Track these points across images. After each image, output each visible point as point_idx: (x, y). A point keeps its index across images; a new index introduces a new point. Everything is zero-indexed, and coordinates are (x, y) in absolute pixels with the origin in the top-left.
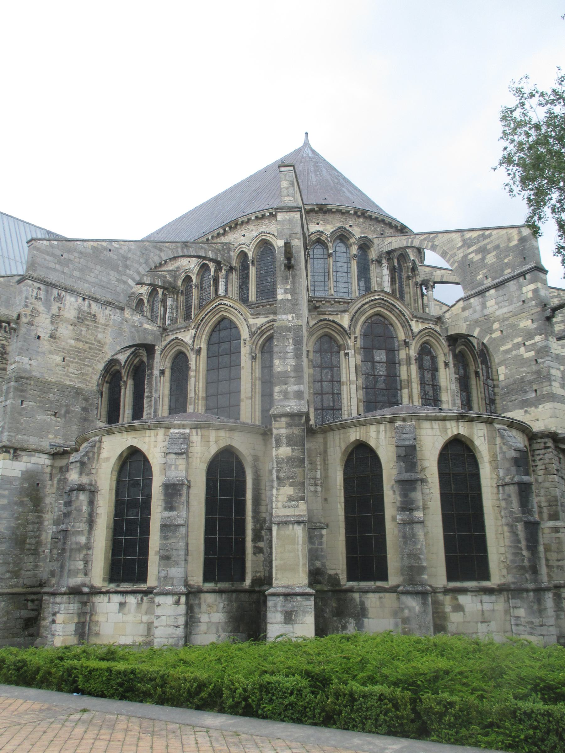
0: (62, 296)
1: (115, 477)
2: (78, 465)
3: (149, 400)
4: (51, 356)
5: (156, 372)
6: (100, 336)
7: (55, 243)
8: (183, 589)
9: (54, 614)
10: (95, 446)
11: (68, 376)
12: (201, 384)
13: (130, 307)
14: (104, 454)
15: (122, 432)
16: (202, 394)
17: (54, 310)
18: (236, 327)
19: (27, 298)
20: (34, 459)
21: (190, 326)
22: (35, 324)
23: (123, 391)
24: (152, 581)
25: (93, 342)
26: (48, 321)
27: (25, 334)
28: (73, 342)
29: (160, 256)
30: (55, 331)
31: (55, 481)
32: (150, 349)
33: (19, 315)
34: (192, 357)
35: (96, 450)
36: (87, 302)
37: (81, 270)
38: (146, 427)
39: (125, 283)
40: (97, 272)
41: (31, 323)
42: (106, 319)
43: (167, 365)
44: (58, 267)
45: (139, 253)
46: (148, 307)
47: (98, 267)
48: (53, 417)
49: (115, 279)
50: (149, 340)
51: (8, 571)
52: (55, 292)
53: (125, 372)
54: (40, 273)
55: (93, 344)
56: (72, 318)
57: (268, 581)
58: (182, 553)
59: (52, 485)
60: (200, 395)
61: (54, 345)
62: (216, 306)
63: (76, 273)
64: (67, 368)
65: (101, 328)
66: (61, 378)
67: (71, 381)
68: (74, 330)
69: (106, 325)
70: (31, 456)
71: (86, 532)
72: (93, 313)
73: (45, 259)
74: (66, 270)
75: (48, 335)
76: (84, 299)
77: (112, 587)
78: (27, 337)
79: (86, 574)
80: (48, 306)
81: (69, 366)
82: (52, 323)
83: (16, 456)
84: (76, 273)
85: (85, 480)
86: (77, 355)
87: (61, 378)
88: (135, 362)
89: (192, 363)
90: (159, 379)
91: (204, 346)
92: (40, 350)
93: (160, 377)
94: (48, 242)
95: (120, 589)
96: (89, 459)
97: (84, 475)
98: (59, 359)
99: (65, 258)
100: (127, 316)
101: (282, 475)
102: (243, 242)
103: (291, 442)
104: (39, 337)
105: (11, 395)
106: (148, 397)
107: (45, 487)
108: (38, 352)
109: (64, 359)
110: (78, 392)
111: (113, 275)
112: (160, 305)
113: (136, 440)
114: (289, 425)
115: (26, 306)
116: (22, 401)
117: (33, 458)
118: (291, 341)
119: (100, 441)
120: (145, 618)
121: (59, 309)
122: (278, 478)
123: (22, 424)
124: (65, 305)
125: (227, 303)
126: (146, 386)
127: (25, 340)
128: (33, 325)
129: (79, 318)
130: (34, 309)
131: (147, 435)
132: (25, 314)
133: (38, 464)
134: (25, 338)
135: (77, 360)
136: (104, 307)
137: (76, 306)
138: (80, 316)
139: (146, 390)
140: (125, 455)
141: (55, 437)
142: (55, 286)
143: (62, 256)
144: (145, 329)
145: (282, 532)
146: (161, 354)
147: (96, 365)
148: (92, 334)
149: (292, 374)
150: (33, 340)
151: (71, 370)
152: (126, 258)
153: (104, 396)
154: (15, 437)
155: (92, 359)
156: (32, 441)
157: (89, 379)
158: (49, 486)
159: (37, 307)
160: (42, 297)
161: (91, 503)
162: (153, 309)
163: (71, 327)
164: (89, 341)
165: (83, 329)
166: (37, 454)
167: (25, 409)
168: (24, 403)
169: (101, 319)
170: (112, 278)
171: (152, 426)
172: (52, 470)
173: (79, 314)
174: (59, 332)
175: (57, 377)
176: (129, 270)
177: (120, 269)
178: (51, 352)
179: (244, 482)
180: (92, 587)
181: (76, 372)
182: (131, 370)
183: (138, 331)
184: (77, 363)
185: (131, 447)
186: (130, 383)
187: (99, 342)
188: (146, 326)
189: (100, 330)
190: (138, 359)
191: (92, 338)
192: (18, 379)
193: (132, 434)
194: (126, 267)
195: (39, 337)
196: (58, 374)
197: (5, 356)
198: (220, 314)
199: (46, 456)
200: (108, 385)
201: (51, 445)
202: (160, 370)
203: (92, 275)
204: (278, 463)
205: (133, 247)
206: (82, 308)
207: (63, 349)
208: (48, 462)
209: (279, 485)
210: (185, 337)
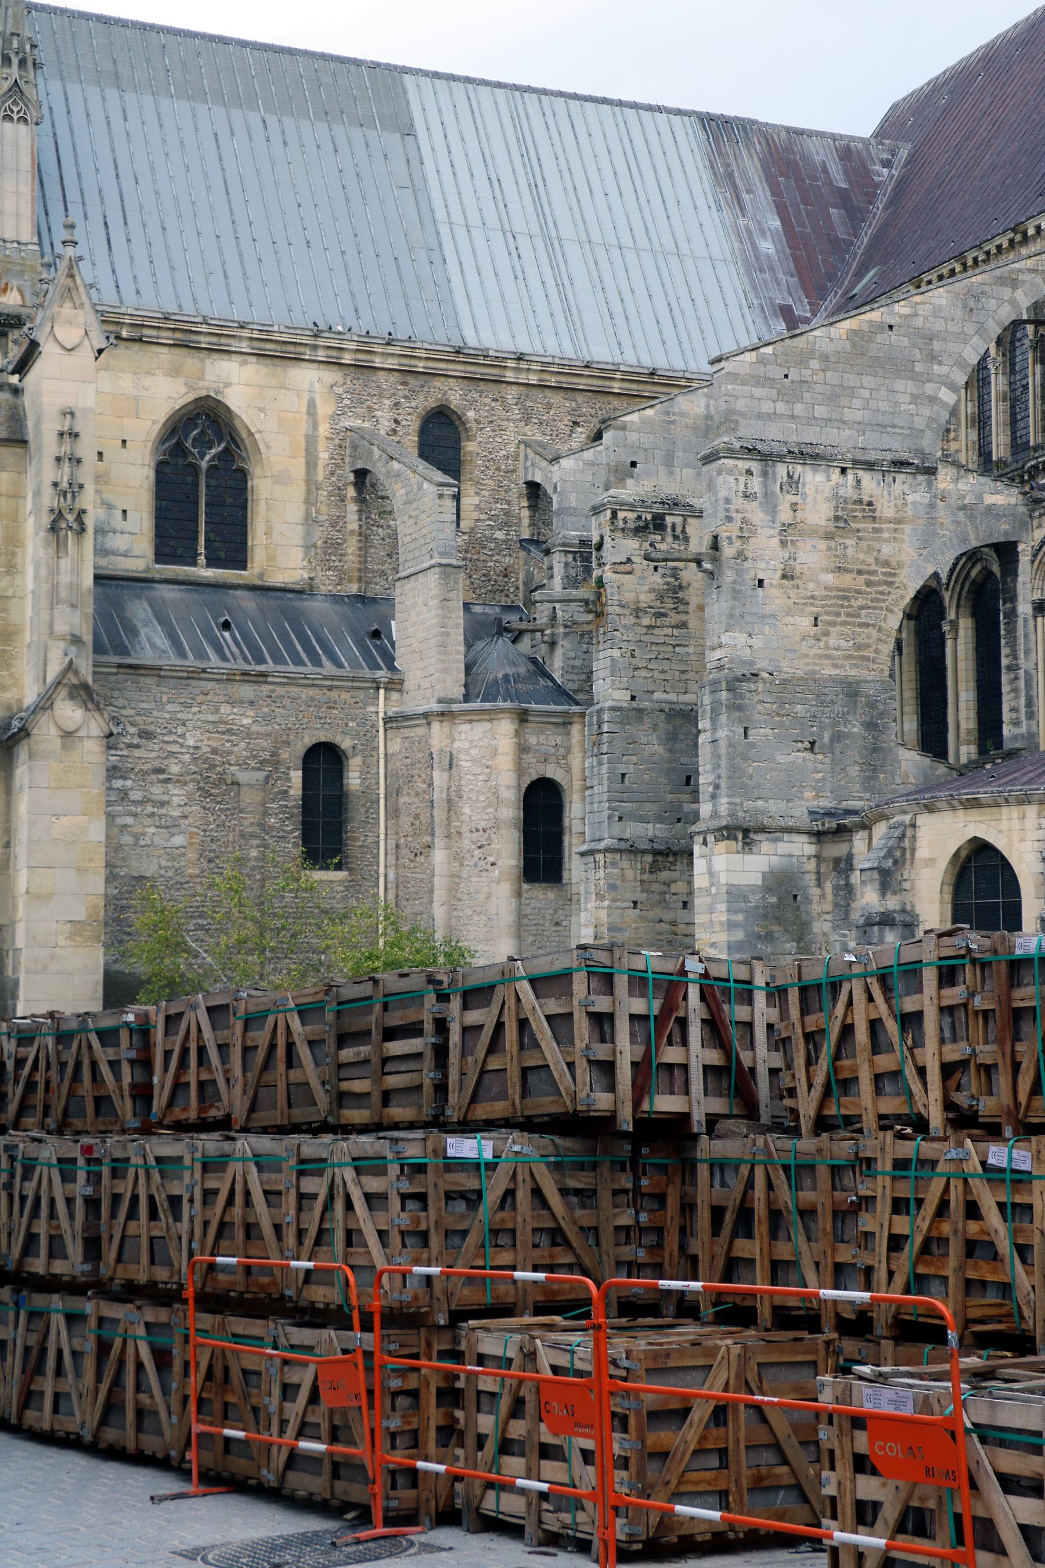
0: (796, 477)
1: (948, 898)
2: (876, 875)
3: (1012, 676)
4: (789, 619)
6: (887, 549)
7: (769, 350)
10: (904, 836)
13: (949, 459)
14: (923, 852)
15: (954, 809)
17: (785, 515)
20: (782, 847)
22: (749, 555)
23: (949, 644)
25: (874, 567)
26: (775, 542)
27: (734, 582)
28: (830, 578)
29: (1013, 302)
30: (791, 562)
31: (828, 887)
32: (1007, 551)
33: (716, 537)
35: (907, 844)
36: (850, 476)
37: (832, 399)
38: (1001, 800)
39: (933, 399)
41: (741, 556)
42: (896, 506)
44: (781, 407)
45: (959, 313)
46: (1000, 359)
47: (868, 381)
48: (808, 755)
49: (908, 398)
50: (1002, 530)
52: (781, 470)
53: (951, 597)
54: (749, 431)
55: (873, 573)
56: (823, 523)
59: (823, 896)
61: (793, 593)
63: (820, 411)
64: (824, 639)
65: (888, 530)
66: (815, 664)
67: (835, 666)
68: (829, 549)
69: (898, 521)
70: (775, 840)
72: (866, 499)
73: (752, 397)
74: (799, 409)
75: (779, 573)
76: (843, 471)
78: (737, 587)
80: (770, 504)
81: (827, 634)
83: (748, 844)
84: (820, 411)
85: (892, 903)
86: (842, 606)
87: (815, 664)
88: (973, 574)
90: (1031, 622)
92: (768, 610)
93: (1035, 618)
94: (754, 353)
96: (895, 862)
97: (889, 896)
98: (806, 622)
99: (792, 382)
100: (942, 486)
104: (761, 583)
106: (1010, 668)
107: (808, 900)
108: (764, 617)
109: (816, 619)
110: (852, 690)
111: (904, 386)
112: (1030, 360)
113: (983, 827)
115: (729, 519)
116: (746, 729)
117: (780, 844)
119: (913, 825)
123: (751, 777)
124: (804, 496)
126: (1003, 642)
127: (736, 594)
128: (746, 559)
129: (837, 518)
130: (744, 521)
131: (1004, 817)
132: (729, 538)
133: (790, 856)
134: (735, 591)
135: (843, 618)
136: (889, 479)
137: (828, 492)
138: (839, 513)
139: (1005, 651)
140: (964, 854)
141: (817, 796)
142: (781, 458)
143: (786, 376)
144: (990, 508)
146: (1033, 562)
147: (885, 620)
148: (870, 549)
150: (750, 593)
151: (833, 642)
153: (905, 650)
154: (741, 804)
155: (875, 608)
156: (773, 809)
157: (872, 655)
158: (816, 899)
159: (748, 516)
160: (756, 489)
162: (1013, 365)
163: (822, 545)
164: (864, 567)
165: (848, 542)
166: (786, 837)
167: (752, 746)
168: (750, 732)
169: (886, 509)
170: (902, 398)
171: (1012, 799)
172: (818, 865)
173: (836, 508)
174: (798, 561)
175: (807, 664)
176: (940, 363)
177: (919, 367)
178: (789, 613)
181: (843, 644)
182: (964, 593)
183: (971, 517)
184: (844, 623)
185: (975, 839)
186: (966, 627)
187: (887, 563)
188: (990, 499)
189: (885, 535)
190: (978, 567)
191: (872, 561)
192: (734, 684)
193: (974, 815)
194: (933, 357)
195: (761, 583)
196: (806, 656)
197: (680, 595)
199: (805, 838)
200: (912, 622)
201: (811, 813)
202: (1033, 602)
203: (857, 403)
205: (944, 301)
206: (842, 492)
207: (812, 597)
208: (810, 849)
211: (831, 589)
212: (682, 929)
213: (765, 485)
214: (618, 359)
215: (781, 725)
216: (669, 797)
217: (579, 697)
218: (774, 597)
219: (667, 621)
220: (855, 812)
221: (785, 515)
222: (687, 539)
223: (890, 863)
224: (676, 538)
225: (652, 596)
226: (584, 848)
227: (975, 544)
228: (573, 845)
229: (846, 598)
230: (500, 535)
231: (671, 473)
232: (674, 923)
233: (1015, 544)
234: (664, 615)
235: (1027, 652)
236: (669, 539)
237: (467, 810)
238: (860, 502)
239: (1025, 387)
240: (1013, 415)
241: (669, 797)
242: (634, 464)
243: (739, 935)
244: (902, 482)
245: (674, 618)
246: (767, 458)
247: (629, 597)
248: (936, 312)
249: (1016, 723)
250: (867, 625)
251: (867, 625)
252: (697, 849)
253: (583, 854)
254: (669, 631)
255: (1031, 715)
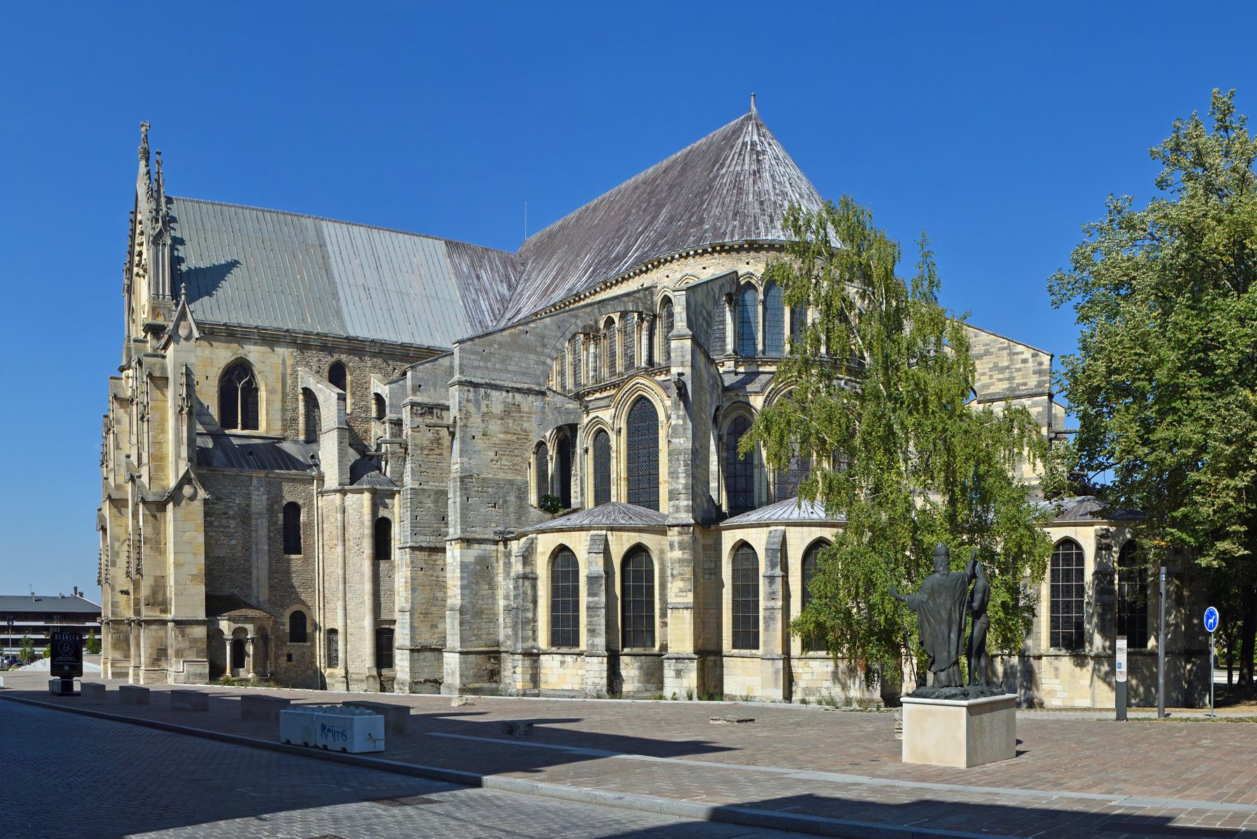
5: (579, 450)
6: (525, 425)
8: (606, 654)
9: (514, 667)
11: (501, 469)
12: (623, 465)
14: (540, 549)
16: (624, 474)
17: (484, 409)
18: (653, 407)
19: (460, 403)
21: (610, 406)
24: (583, 646)
26: (479, 420)
28: (502, 436)
32: (573, 428)
34: (613, 436)
36: (511, 394)
37: (503, 361)
40: (517, 359)
41: (465, 426)
43: (589, 443)
44: (482, 364)
47: (517, 354)
51: (474, 635)
52: (482, 391)
55: (520, 434)
56: (499, 412)
57: (664, 647)
58: (604, 627)
60: (622, 475)
61: (487, 442)
62: (634, 385)
63: (498, 366)
68: (502, 424)
69: (530, 413)
71: (531, 610)
72: (517, 403)
74: (489, 365)
77: (554, 649)
79: (535, 640)
80: (478, 406)
81: (501, 459)
82: (483, 421)
84: (498, 366)
85: (528, 570)
89: (613, 444)
91: (623, 425)
92: (476, 448)
95: (560, 651)
98: (493, 454)
101: (675, 572)
102: (666, 284)
103: (682, 546)
105: (458, 493)
108: (475, 452)
111: (533, 357)
114: (680, 533)
118: (682, 462)
119: (536, 538)
120: (580, 672)
121: (487, 405)
122: (672, 575)
125: (644, 382)
129: (505, 411)
141: (497, 526)
145: (674, 615)
148: (519, 424)
149: (683, 491)
151: (503, 463)
152: (543, 337)
161: (534, 587)
162: (575, 351)
163: (499, 422)
169: (525, 408)
177: (538, 349)
179: (653, 571)
180: (538, 649)
181: (507, 463)
184: (508, 455)
185: (561, 544)
187: (525, 431)
191: (519, 429)
194: (544, 346)
195: (474, 437)
198: (638, 393)
203: (513, 363)
204: (672, 563)
206: (507, 400)
209: (673, 580)
210: (605, 415)
211: (503, 440)
212: (441, 579)
213: (475, 396)
214: (413, 342)
215: (482, 496)
216: (435, 526)
217: (398, 483)
218: (480, 443)
219: (434, 452)
220: (513, 533)
221: (484, 409)
222: (442, 419)
223: (527, 554)
224: (438, 417)
225: (428, 442)
226: (400, 546)
227: (561, 424)
228: (395, 543)
229: (509, 445)
230: (363, 415)
231: (436, 390)
232: (437, 577)
233: (577, 424)
234: (433, 450)
235: (581, 469)
236: (435, 418)
237: (351, 530)
238: (514, 404)
239: (580, 360)
240: (575, 371)
241: (435, 526)
242: (420, 386)
243: (465, 582)
244: (531, 398)
245: (437, 451)
246: (476, 386)
247: (418, 442)
248: (545, 326)
249: (576, 498)
250: (517, 456)
251: (517, 456)
252: (448, 547)
253: (400, 549)
254: (435, 457)
255: (582, 495)
